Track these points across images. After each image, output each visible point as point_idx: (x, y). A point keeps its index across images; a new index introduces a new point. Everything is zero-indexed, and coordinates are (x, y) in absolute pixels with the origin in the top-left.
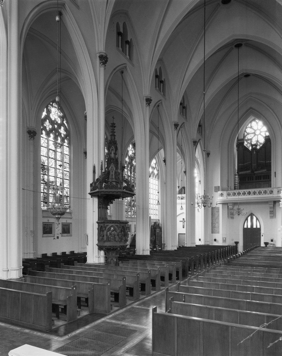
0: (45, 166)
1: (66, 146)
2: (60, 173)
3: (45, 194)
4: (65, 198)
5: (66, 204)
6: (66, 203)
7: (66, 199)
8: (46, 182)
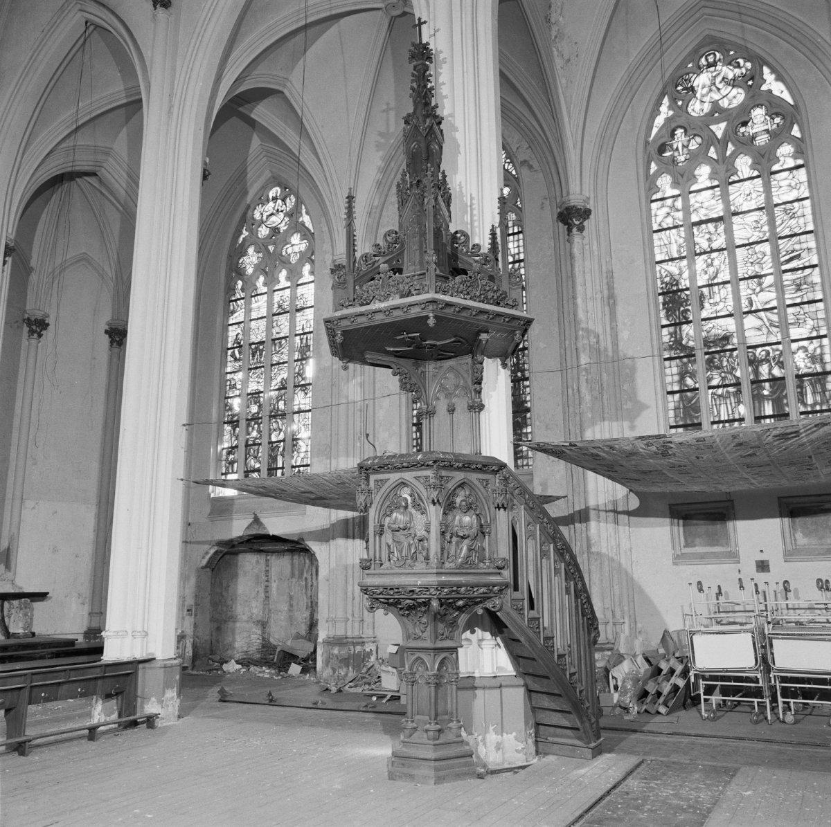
0: (683, 290)
1: (791, 169)
2: (762, 290)
3: (689, 394)
4: (806, 384)
5: (818, 408)
6: (815, 404)
7: (814, 388)
8: (692, 349)
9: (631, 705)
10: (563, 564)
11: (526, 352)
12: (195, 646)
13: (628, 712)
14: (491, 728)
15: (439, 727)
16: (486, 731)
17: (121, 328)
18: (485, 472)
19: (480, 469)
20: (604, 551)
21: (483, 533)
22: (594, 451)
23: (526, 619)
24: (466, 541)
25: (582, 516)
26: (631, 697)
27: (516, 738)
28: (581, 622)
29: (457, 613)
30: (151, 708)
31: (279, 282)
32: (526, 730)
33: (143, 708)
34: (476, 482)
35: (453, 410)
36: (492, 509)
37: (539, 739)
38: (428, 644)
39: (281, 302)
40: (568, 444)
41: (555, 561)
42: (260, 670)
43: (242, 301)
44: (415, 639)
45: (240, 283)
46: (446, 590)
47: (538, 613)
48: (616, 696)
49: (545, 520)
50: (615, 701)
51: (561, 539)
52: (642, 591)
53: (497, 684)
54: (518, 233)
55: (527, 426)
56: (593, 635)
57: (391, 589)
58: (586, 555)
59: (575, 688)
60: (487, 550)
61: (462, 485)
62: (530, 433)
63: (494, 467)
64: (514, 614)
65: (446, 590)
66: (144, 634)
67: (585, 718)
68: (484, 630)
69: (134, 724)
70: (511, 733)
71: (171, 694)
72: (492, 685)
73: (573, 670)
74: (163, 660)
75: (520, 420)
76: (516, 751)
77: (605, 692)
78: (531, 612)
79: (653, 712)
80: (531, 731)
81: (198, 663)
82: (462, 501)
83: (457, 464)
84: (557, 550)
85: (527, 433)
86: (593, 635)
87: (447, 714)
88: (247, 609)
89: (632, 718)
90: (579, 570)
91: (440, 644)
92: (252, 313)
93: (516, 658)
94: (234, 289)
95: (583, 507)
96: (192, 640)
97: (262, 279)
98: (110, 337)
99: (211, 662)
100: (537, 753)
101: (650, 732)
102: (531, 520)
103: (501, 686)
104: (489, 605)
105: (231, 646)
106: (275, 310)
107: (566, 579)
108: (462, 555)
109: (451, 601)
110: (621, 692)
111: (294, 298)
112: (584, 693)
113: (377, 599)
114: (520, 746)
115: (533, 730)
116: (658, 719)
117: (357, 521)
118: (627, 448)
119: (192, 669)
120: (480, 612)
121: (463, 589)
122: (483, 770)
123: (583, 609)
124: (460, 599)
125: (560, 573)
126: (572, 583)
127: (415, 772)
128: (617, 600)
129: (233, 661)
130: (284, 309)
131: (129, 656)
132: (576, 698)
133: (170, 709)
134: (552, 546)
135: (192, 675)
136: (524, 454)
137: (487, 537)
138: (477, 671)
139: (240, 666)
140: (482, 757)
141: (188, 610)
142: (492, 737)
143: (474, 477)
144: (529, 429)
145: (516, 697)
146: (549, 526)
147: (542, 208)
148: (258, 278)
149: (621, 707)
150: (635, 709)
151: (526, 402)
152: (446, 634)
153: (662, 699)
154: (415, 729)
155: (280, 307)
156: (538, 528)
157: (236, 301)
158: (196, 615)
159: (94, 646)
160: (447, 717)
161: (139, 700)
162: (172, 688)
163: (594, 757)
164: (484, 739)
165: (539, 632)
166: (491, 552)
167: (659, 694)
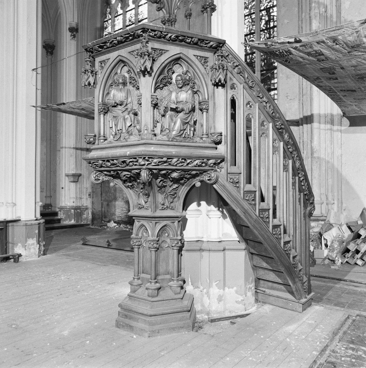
9: (337, 259)
10: (282, 144)
11: (275, 29)
12: (93, 214)
13: (334, 263)
14: (214, 284)
15: (158, 285)
16: (210, 286)
17: (51, 44)
18: (202, 48)
19: (196, 44)
20: (322, 156)
21: (201, 110)
22: (317, 48)
23: (242, 192)
24: (181, 115)
25: (308, 120)
26: (337, 253)
27: (237, 292)
28: (298, 197)
29: (176, 186)
30: (18, 250)
31: (129, 6)
32: (245, 285)
33: (13, 249)
34: (194, 59)
35: (190, 15)
36: (211, 87)
37: (258, 291)
38: (148, 213)
39: (130, 18)
40: (292, 40)
41: (274, 141)
42: (125, 226)
43: (110, 21)
44: (140, 208)
45: (108, 10)
46: (155, 160)
47: (254, 186)
48: (326, 252)
49: (265, 99)
50: (325, 255)
51: (279, 118)
52: (348, 183)
53: (222, 248)
55: (274, 78)
56: (309, 209)
57: (108, 161)
58: (310, 159)
59: (288, 255)
60: (205, 127)
61: (177, 60)
62: (276, 83)
63: (212, 43)
64: (230, 187)
65: (155, 160)
66: (12, 204)
67: (297, 280)
68: (209, 204)
69: (7, 259)
70: (233, 288)
71: (32, 242)
72: (216, 248)
73: (287, 239)
74: (26, 221)
76: (236, 302)
77: (318, 248)
78: (248, 185)
79: (352, 263)
80: (251, 286)
81: (95, 222)
82: (177, 76)
83: (169, 35)
84: (275, 128)
85: (274, 84)
86: (309, 209)
87: (169, 274)
88: (121, 195)
89: (337, 268)
90: (297, 149)
91: (159, 213)
92: (116, 27)
93: (240, 227)
94: (106, 14)
95: (309, 114)
96: (91, 210)
97: (120, 5)
98: (46, 50)
99: (103, 222)
100: (257, 301)
101: (351, 281)
102: (251, 99)
103: (224, 250)
104: (205, 178)
105: (114, 214)
106: (128, 23)
107: (284, 157)
108: (176, 128)
109: (164, 172)
110: (330, 250)
111: (137, 14)
112: (298, 258)
113: (101, 171)
114: (240, 298)
115: (253, 284)
116: (356, 268)
117: (83, 97)
118: (351, 38)
119: (92, 225)
120: (198, 184)
121: (175, 160)
122: (206, 317)
123: (300, 186)
124: (174, 171)
125: (279, 152)
126: (290, 161)
127: (133, 323)
128: (330, 188)
129: (112, 222)
130: (132, 22)
131: (10, 218)
132: (290, 263)
133: (32, 250)
134: (271, 125)
135: (92, 228)
137: (205, 113)
138: (205, 236)
139: (116, 224)
140: (206, 305)
141: (89, 195)
142: (215, 291)
143: (191, 53)
144: (276, 81)
145: (239, 258)
146: (268, 105)
148: (118, 5)
149: (329, 259)
150: (339, 261)
152: (167, 204)
153: (360, 255)
154: (140, 285)
155: (130, 21)
156: (257, 107)
157: (107, 21)
158: (93, 198)
159: (49, 212)
160: (168, 277)
161: (10, 245)
162: (33, 238)
163: (304, 310)
164: (208, 293)
165: (255, 205)
166: (208, 128)
167: (357, 252)
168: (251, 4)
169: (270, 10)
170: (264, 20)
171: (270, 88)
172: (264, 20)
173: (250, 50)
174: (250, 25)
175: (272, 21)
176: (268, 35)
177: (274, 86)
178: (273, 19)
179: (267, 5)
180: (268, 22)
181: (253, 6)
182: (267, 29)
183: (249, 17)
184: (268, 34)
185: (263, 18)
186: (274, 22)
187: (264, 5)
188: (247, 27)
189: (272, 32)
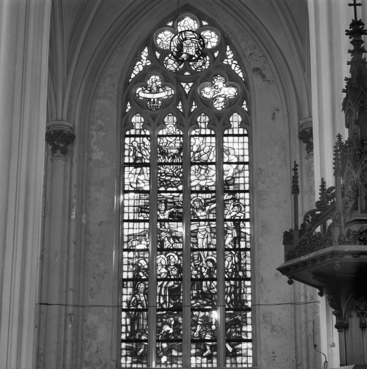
54: (243, 135)
75: (240, 318)
136: (244, 352)
147: (273, 118)
151: (247, 301)
168: (210, 205)
169: (240, 224)
170: (230, 236)
171: (241, 336)
172: (230, 236)
173: (207, 273)
174: (208, 236)
175: (242, 239)
176: (237, 259)
177: (247, 336)
178: (245, 238)
179: (235, 216)
180: (236, 240)
181: (212, 209)
182: (234, 249)
183: (207, 223)
184: (237, 257)
185: (229, 231)
186: (246, 242)
187: (230, 213)
188: (202, 237)
189: (242, 256)
